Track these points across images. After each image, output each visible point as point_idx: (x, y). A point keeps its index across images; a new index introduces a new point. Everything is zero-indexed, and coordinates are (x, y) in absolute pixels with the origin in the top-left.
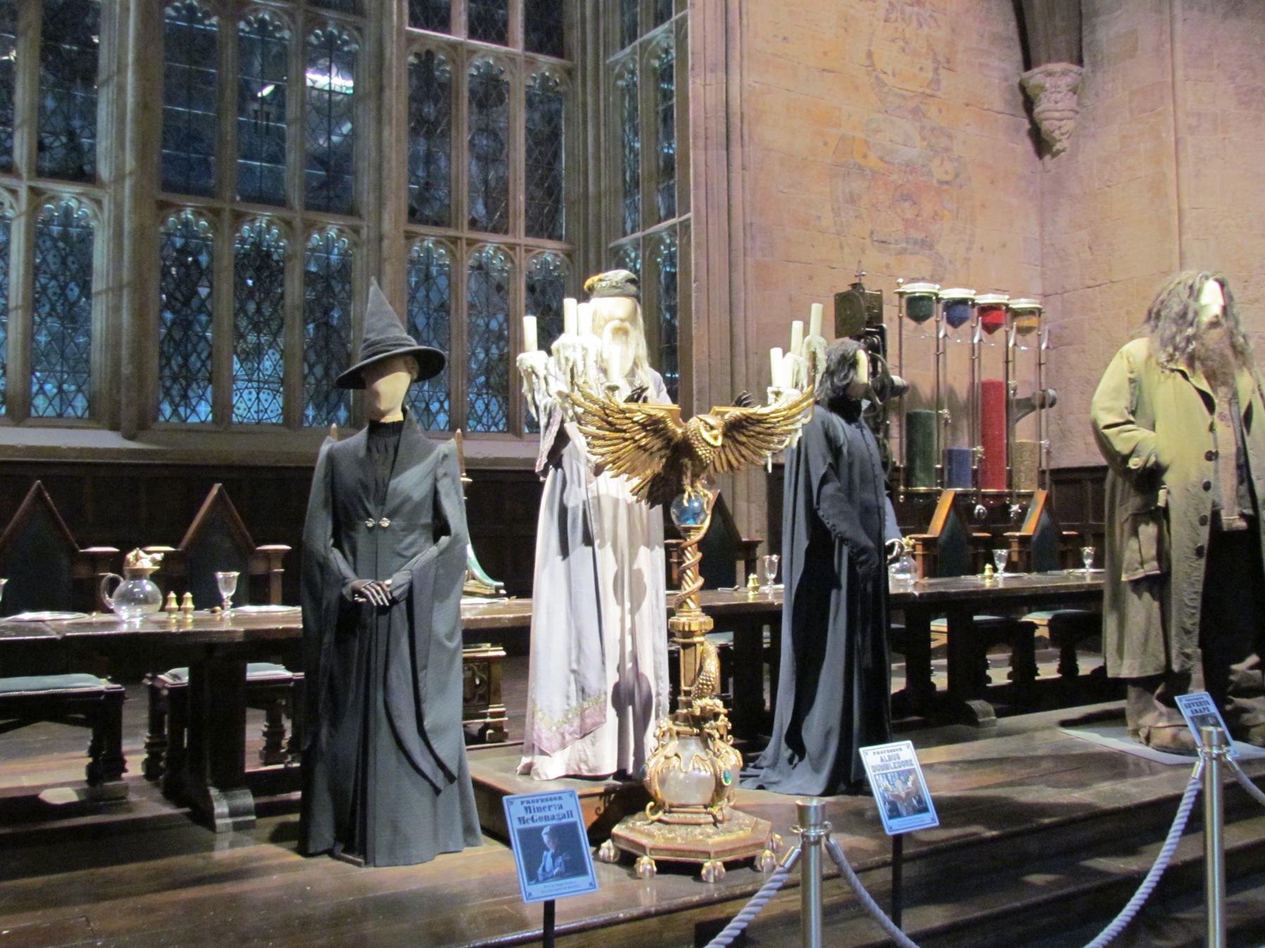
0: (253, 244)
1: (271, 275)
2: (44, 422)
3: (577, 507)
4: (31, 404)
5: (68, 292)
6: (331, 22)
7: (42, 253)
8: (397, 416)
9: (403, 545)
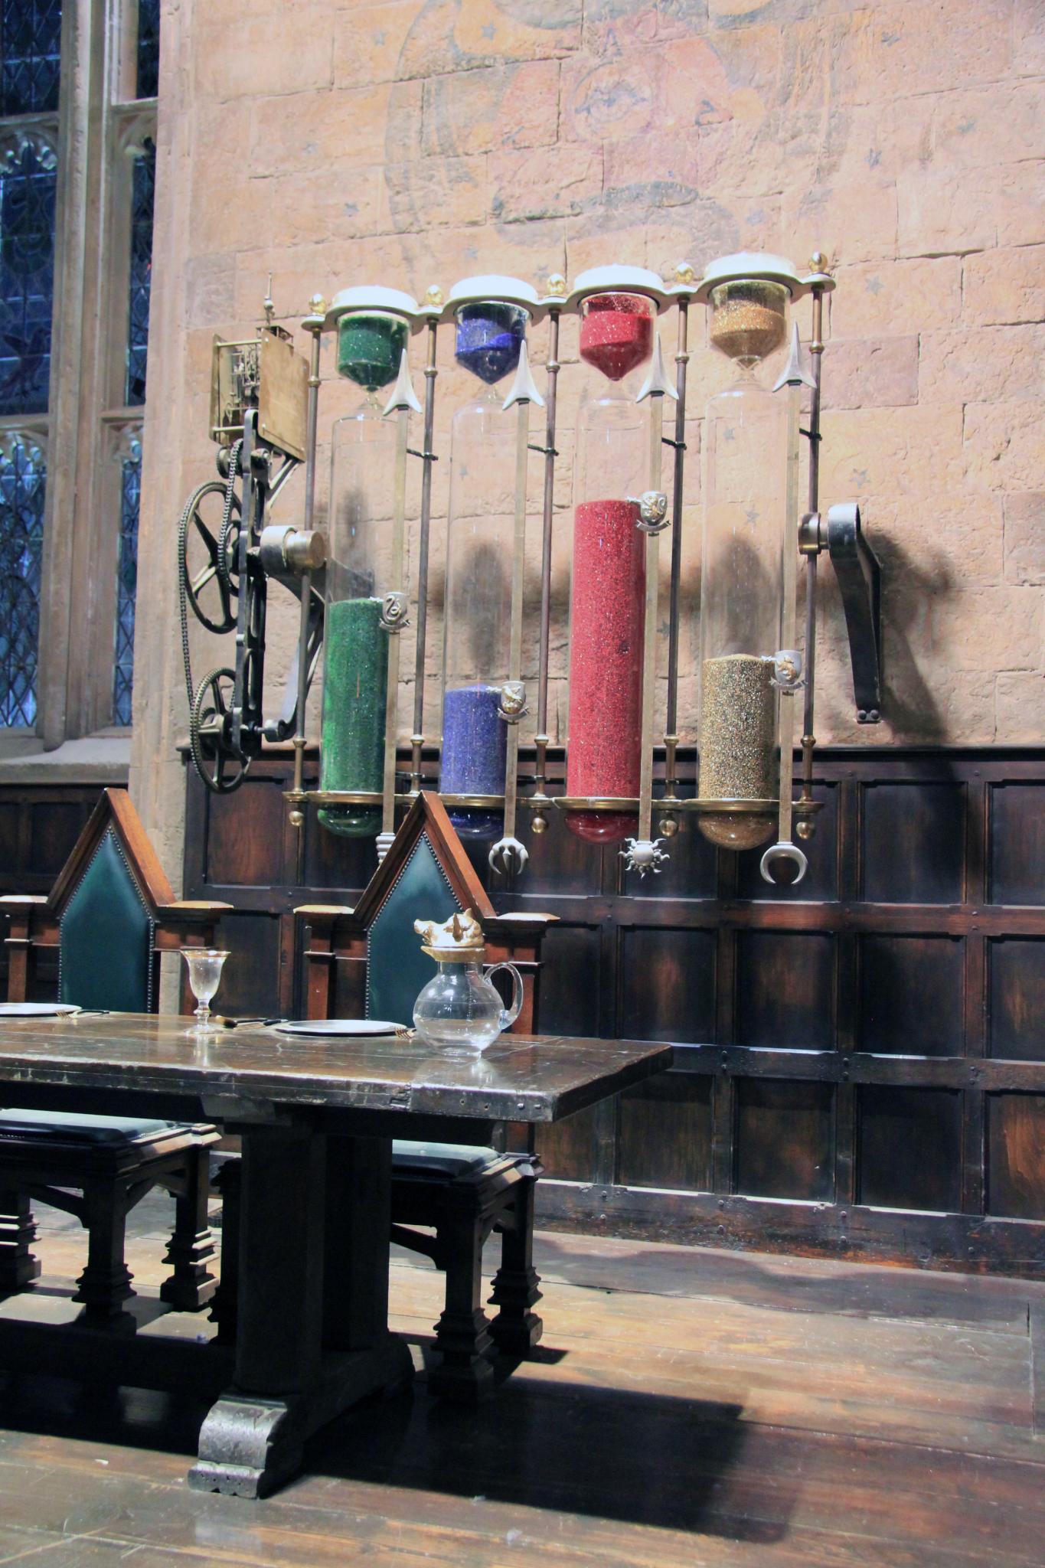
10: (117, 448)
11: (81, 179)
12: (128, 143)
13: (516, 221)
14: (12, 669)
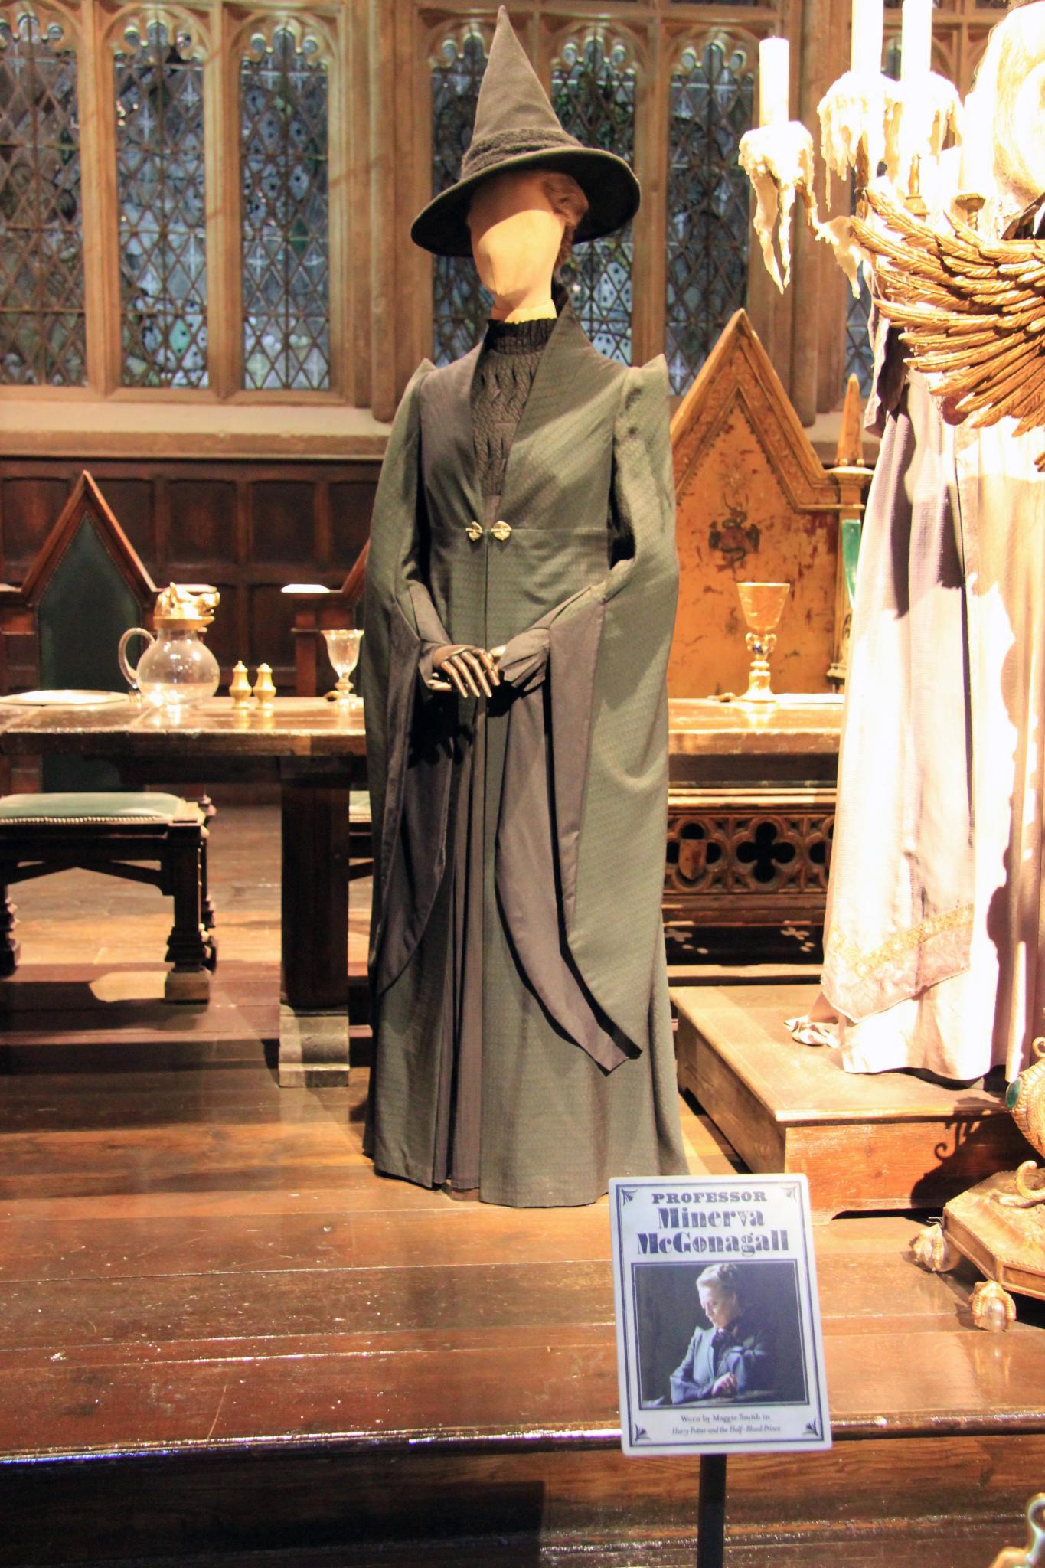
0: (582, 75)
1: (612, 130)
2: (266, 399)
3: (934, 500)
4: (246, 370)
5: (293, 183)
7: (251, 118)
8: (539, 307)
9: (537, 578)
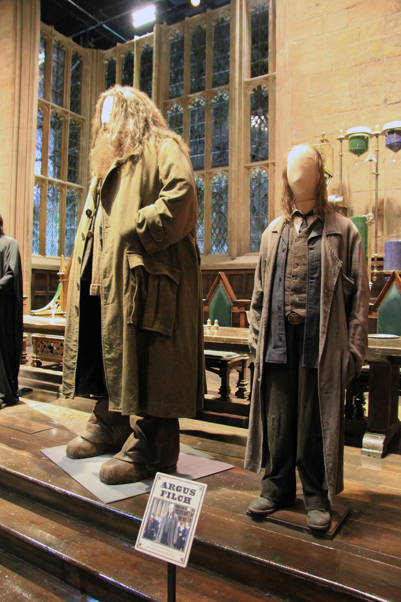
6: (218, 92)
10: (249, 175)
11: (237, 102)
12: (249, 90)
13: (391, 104)
14: (220, 238)
